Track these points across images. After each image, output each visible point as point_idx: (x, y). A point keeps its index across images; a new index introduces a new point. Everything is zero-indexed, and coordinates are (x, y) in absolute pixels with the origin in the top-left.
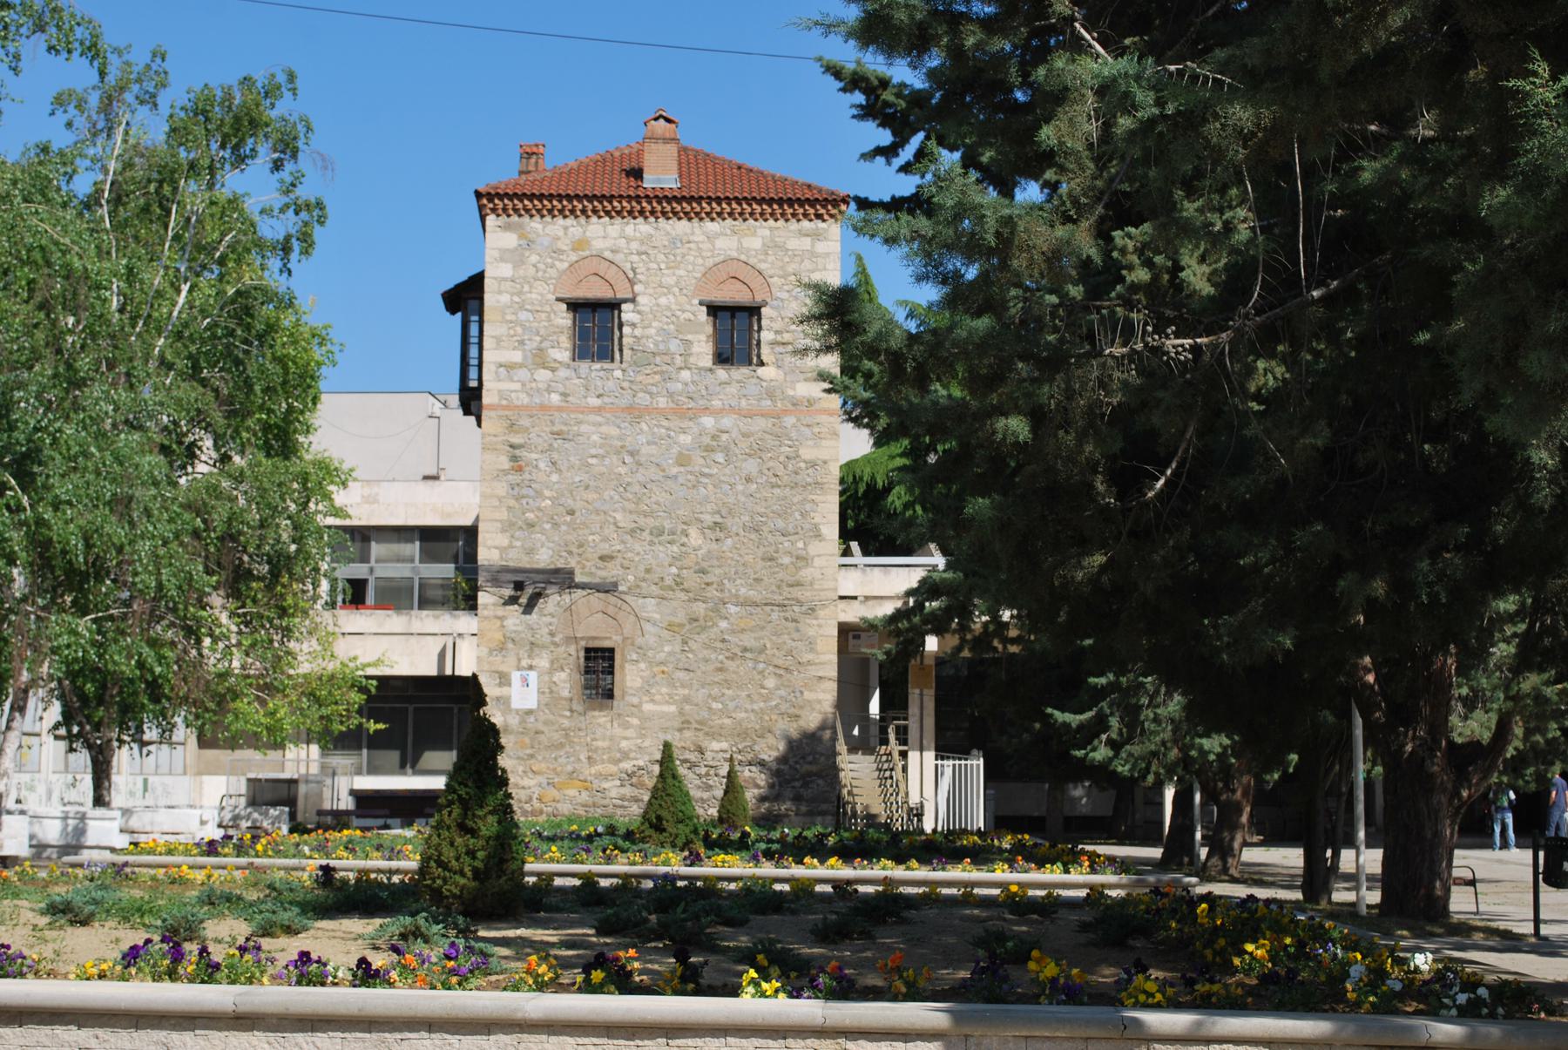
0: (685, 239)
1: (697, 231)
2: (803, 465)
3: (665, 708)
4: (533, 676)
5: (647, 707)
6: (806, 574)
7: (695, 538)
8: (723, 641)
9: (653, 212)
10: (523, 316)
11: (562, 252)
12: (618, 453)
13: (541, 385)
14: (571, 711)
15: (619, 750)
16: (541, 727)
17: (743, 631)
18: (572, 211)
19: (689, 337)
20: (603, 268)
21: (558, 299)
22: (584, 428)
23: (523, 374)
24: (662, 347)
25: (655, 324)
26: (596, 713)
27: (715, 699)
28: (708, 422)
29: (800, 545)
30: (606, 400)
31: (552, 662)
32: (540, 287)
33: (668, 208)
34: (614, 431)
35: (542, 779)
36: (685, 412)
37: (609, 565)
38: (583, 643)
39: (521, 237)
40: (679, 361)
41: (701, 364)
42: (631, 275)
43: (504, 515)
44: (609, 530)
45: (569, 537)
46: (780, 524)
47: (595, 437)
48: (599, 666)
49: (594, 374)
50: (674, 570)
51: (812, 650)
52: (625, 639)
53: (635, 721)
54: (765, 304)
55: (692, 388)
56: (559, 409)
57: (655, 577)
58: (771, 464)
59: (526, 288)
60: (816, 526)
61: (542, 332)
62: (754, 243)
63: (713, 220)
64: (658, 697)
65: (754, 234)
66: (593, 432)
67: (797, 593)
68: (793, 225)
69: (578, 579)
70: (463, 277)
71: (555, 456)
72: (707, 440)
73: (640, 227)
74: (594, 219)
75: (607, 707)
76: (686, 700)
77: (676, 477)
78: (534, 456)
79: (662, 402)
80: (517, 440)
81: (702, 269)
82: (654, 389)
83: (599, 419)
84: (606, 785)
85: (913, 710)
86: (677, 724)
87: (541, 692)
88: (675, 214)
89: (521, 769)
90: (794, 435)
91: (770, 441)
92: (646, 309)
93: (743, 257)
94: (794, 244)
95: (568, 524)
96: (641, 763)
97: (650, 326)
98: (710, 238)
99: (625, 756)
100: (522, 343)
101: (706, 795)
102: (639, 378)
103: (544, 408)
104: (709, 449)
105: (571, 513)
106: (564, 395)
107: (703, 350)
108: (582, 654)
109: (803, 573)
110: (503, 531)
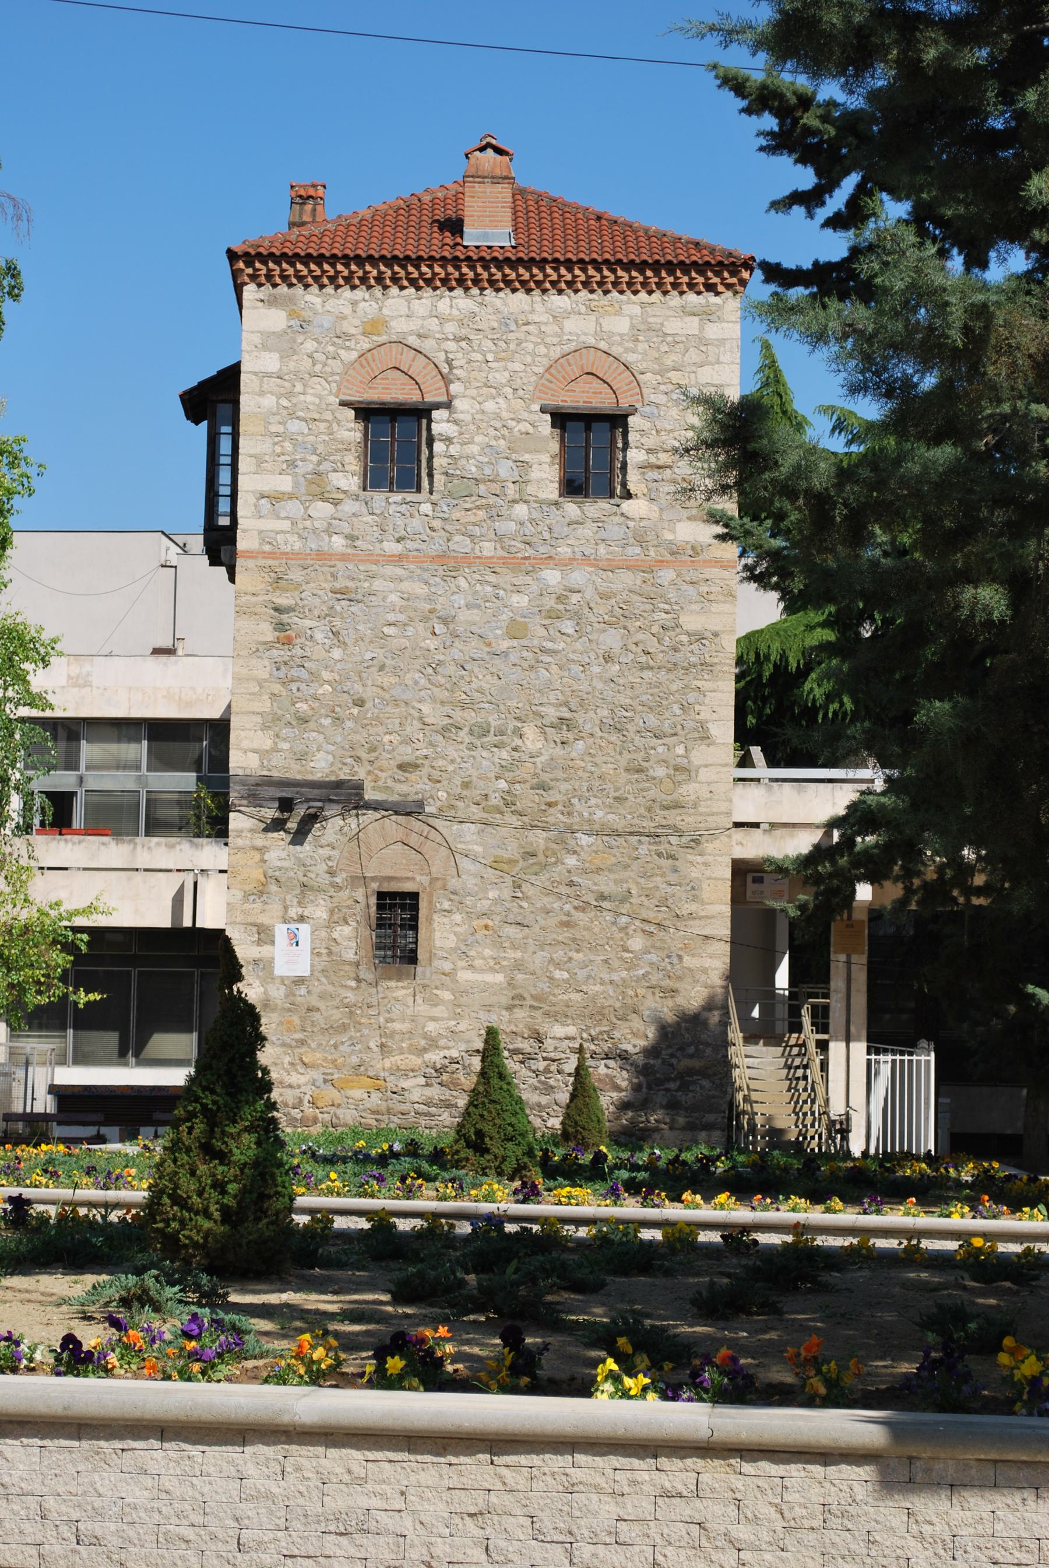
0: (522, 318)
1: (538, 307)
2: (684, 638)
3: (489, 978)
4: (304, 931)
5: (465, 976)
6: (689, 790)
7: (532, 740)
8: (571, 884)
9: (476, 281)
10: (295, 426)
11: (348, 337)
12: (425, 619)
13: (317, 524)
14: (358, 980)
15: (425, 1036)
16: (314, 1001)
17: (599, 870)
18: (364, 280)
19: (527, 457)
20: (406, 359)
21: (343, 404)
22: (378, 584)
23: (293, 508)
24: (488, 471)
25: (479, 439)
26: (393, 984)
27: (558, 966)
28: (552, 577)
29: (680, 750)
30: (410, 545)
31: (332, 912)
32: (318, 386)
33: (499, 276)
34: (420, 589)
35: (316, 1075)
36: (521, 561)
37: (413, 777)
38: (375, 886)
39: (291, 315)
40: (511, 491)
41: (542, 496)
42: (445, 370)
43: (265, 705)
44: (413, 729)
45: (356, 738)
46: (652, 721)
47: (393, 598)
48: (397, 920)
49: (392, 509)
50: (502, 784)
51: (695, 899)
52: (434, 880)
53: (447, 995)
54: (634, 411)
55: (529, 529)
56: (344, 557)
57: (476, 794)
58: (640, 636)
59: (299, 388)
60: (703, 725)
61: (321, 449)
62: (620, 325)
63: (560, 292)
64: (478, 963)
65: (619, 312)
66: (391, 589)
67: (674, 817)
68: (674, 299)
69: (369, 795)
70: (210, 371)
71: (338, 623)
72: (550, 602)
73: (457, 303)
74: (394, 290)
75: (408, 977)
76: (519, 966)
77: (506, 654)
78: (308, 623)
79: (488, 548)
80: (283, 601)
81: (546, 362)
82: (477, 531)
83: (399, 571)
84: (406, 1084)
85: (837, 983)
86: (505, 1000)
87: (315, 953)
88: (508, 283)
89: (287, 1059)
90: (672, 596)
91: (639, 604)
92: (467, 418)
93: (603, 345)
94: (675, 326)
95: (356, 719)
96: (454, 1053)
97: (471, 442)
98: (557, 318)
99: (433, 1043)
100: (292, 464)
101: (544, 1100)
102: (457, 514)
103: (321, 555)
104: (554, 616)
105: (360, 703)
106: (351, 538)
107: (546, 475)
108: (373, 900)
109: (683, 789)
110: (265, 728)
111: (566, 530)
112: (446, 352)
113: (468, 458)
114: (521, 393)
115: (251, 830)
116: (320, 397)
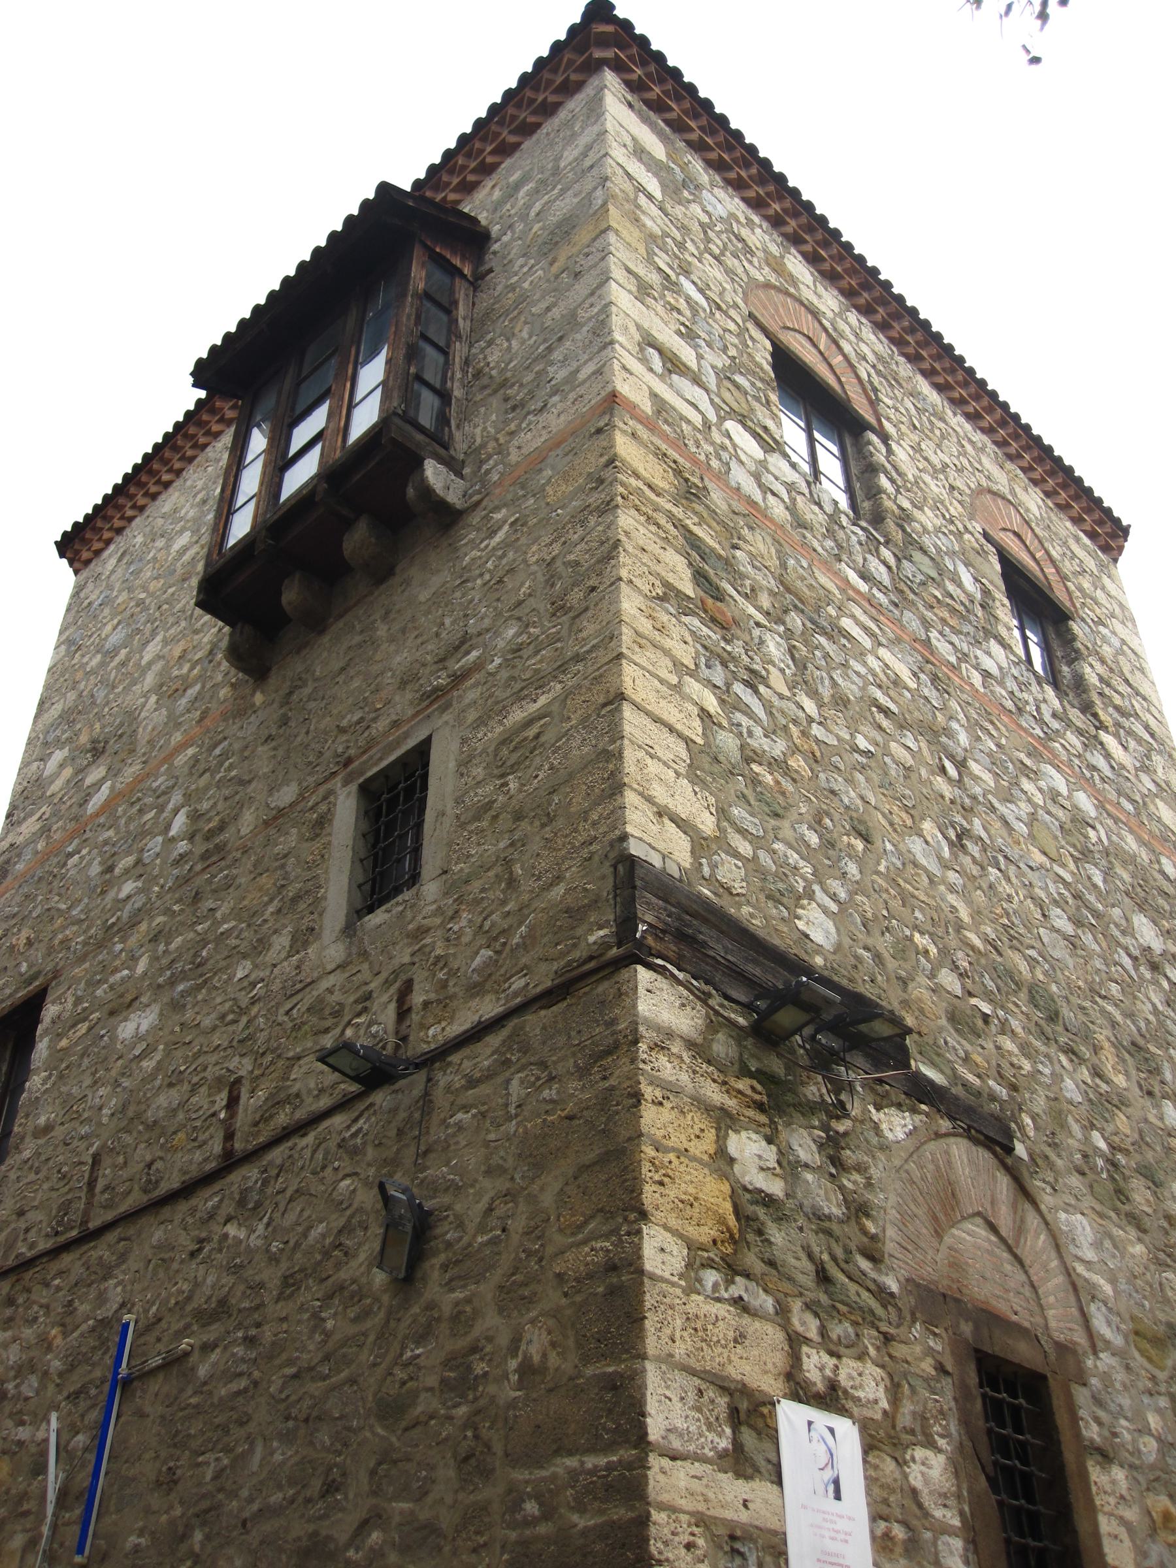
13: (743, 457)
39: (669, 155)
74: (793, 250)
95: (860, 862)
111: (1055, 725)
112: (869, 375)
113: (925, 530)
114: (956, 493)
115: (690, 1044)
116: (724, 289)
